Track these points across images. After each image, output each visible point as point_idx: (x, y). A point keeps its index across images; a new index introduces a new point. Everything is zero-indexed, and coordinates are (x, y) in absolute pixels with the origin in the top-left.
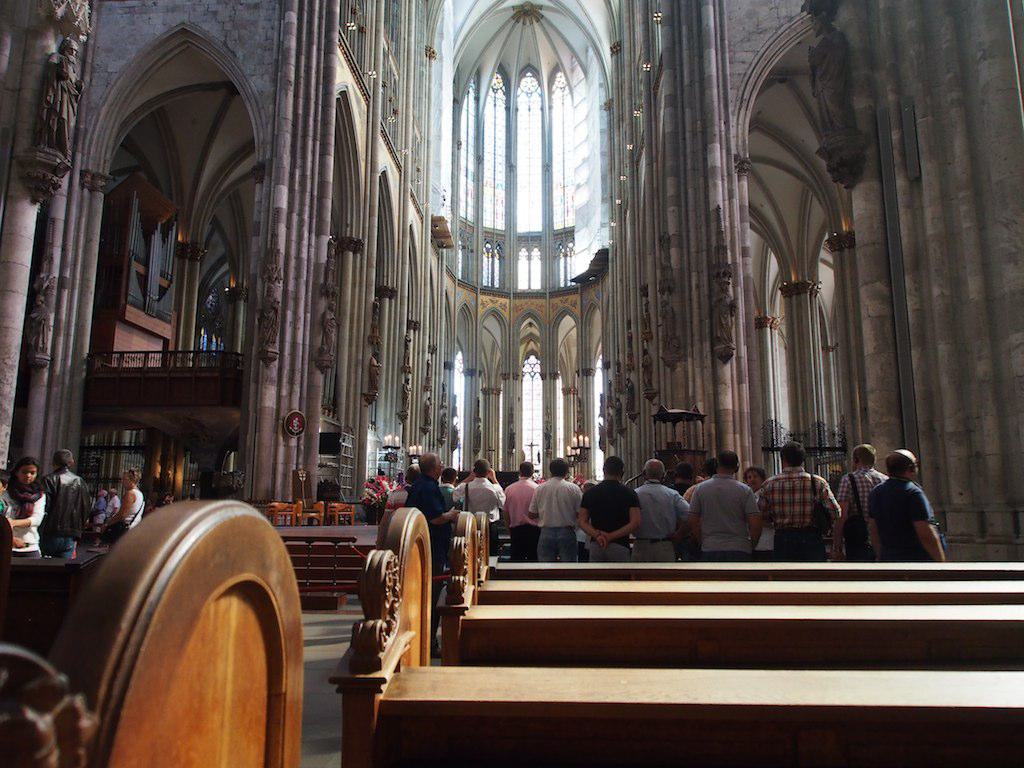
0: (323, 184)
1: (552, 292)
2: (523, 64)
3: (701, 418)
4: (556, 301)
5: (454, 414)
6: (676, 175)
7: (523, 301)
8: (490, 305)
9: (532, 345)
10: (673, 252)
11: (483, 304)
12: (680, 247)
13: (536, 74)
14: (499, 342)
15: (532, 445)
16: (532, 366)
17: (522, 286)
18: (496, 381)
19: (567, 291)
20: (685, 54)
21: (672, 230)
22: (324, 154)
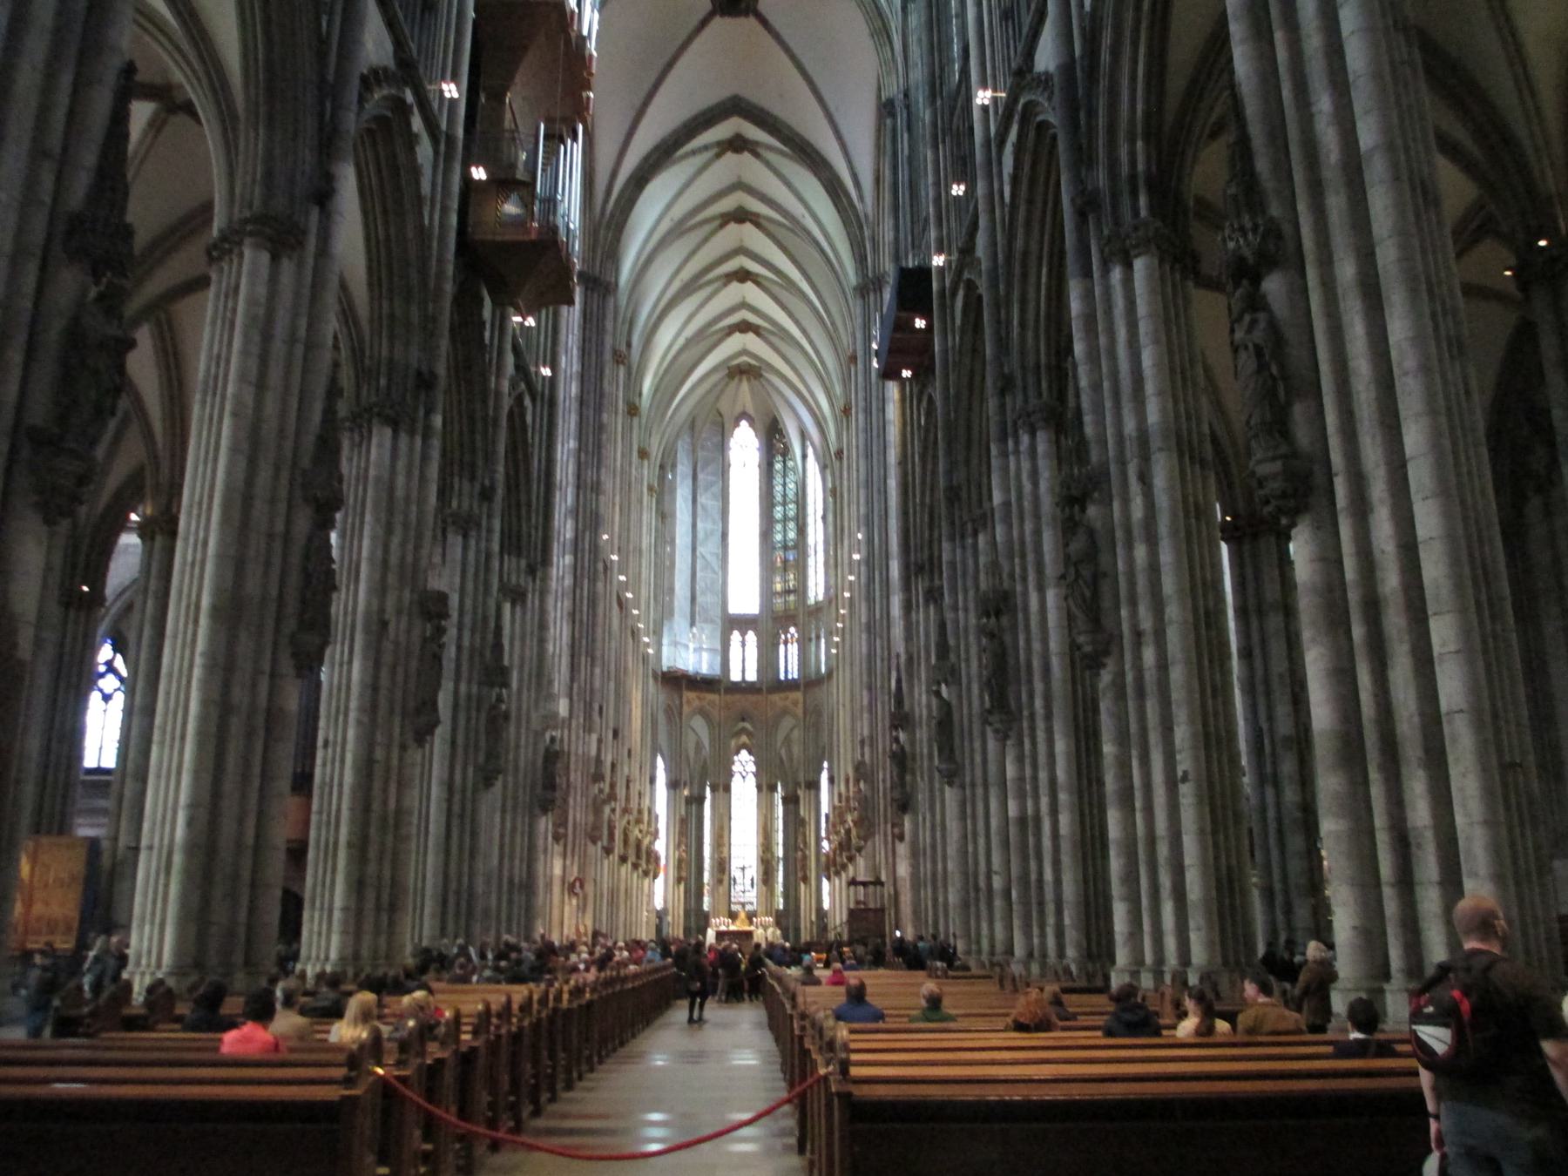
0: (592, 690)
1: (770, 684)
2: (738, 409)
3: (882, 884)
4: (776, 697)
5: (656, 835)
6: (870, 689)
7: (737, 697)
8: (696, 703)
9: (744, 739)
10: (867, 749)
11: (688, 702)
12: (871, 746)
13: (752, 424)
14: (706, 742)
15: (743, 869)
16: (744, 763)
17: (735, 676)
18: (701, 781)
19: (791, 685)
20: (877, 594)
21: (866, 732)
22: (593, 666)
